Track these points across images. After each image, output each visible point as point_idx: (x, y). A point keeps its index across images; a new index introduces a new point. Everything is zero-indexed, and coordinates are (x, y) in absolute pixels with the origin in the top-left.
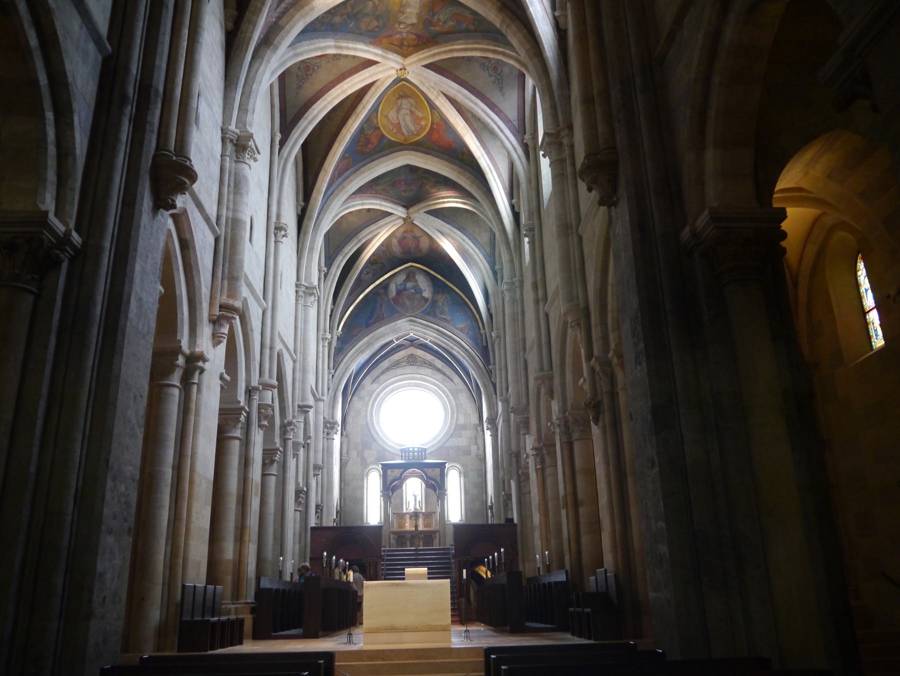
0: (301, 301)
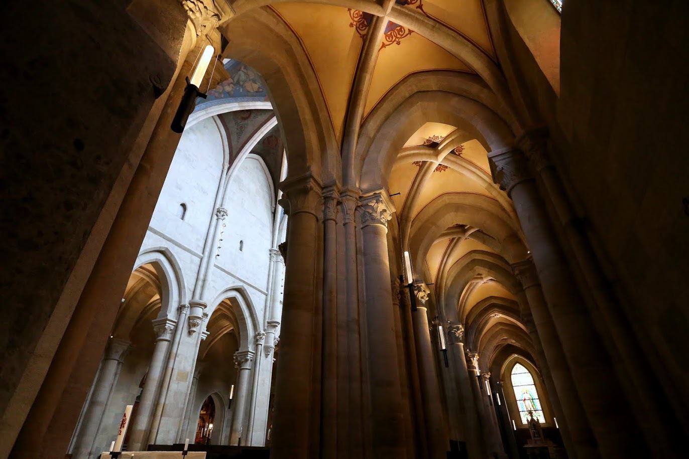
0: (274, 259)
